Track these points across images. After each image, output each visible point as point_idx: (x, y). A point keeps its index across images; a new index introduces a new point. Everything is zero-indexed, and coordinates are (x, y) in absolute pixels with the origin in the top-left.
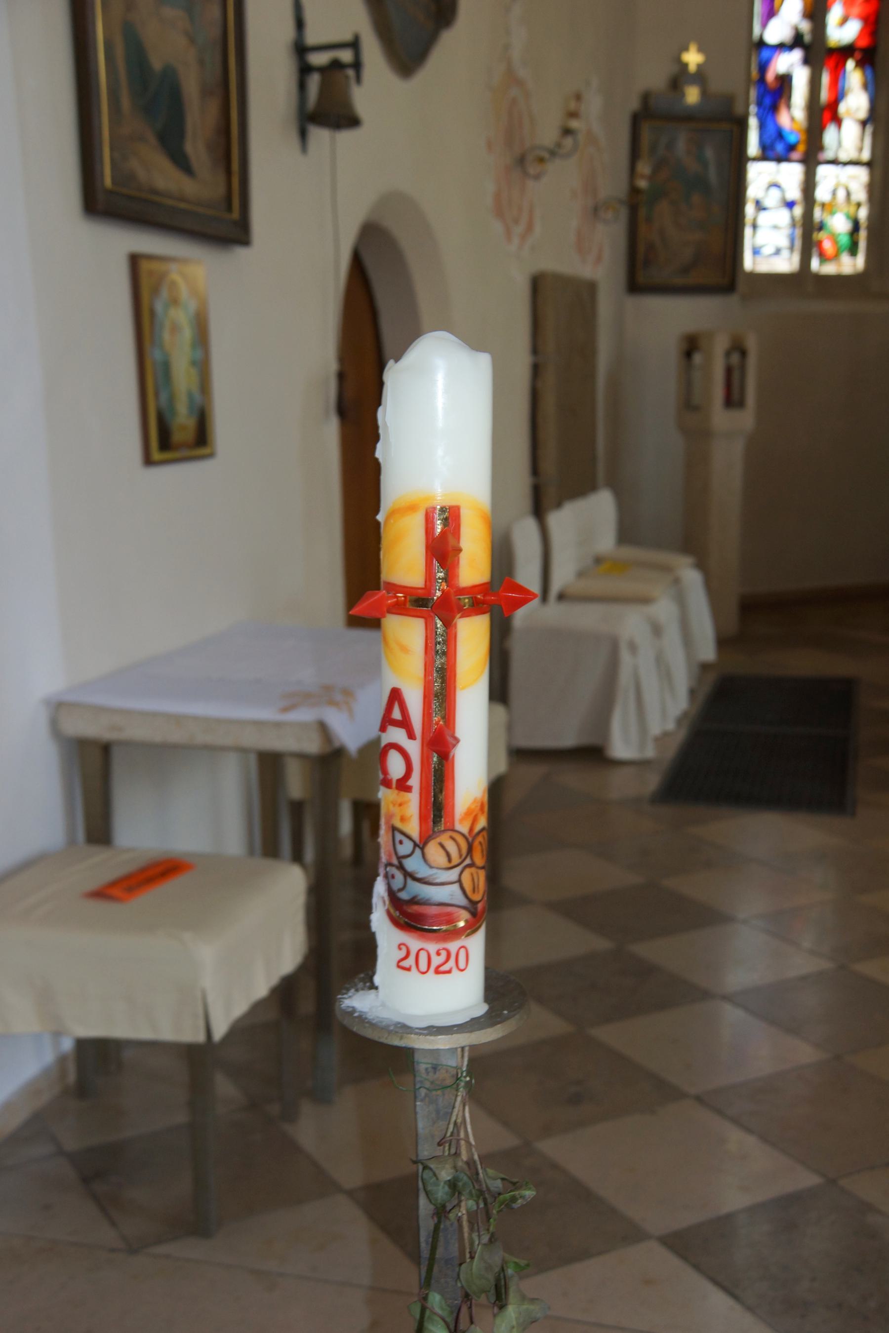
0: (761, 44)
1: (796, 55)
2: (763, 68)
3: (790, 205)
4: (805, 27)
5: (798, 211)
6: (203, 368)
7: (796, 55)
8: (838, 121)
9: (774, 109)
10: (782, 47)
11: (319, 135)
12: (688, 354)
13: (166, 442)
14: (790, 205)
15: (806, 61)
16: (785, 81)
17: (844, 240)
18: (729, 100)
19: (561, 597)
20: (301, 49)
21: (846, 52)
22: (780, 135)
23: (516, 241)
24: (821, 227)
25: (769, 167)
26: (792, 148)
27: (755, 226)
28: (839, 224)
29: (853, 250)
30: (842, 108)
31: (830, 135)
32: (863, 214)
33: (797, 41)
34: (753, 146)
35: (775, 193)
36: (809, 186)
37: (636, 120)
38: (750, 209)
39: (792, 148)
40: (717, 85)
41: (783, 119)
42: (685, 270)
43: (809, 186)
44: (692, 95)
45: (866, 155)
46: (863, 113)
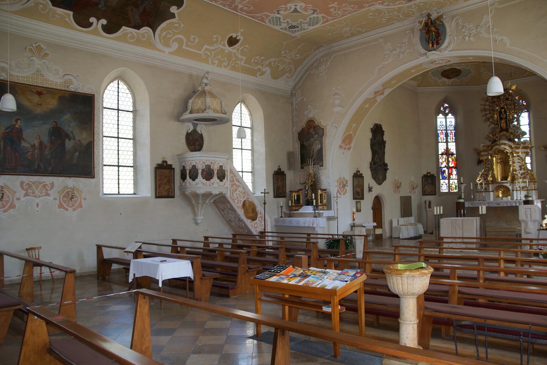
0: (441, 167)
1: (446, 168)
2: (441, 170)
3: (446, 184)
4: (447, 165)
5: (448, 185)
6: (361, 208)
7: (446, 168)
8: (452, 175)
9: (443, 174)
10: (444, 167)
11: (370, 192)
12: (425, 202)
13: (358, 211)
14: (446, 184)
15: (447, 169)
16: (444, 171)
17: (455, 188)
18: (433, 175)
19: (400, 225)
20: (369, 187)
21: (453, 167)
22: (444, 176)
23: (397, 194)
24: (451, 187)
25: (443, 181)
26: (446, 178)
27: (442, 187)
28: (454, 186)
29: (456, 189)
30: (453, 173)
31: (451, 176)
32: (457, 185)
33: (446, 167)
34: (441, 178)
35: (444, 183)
36: (449, 182)
37: (422, 177)
38: (441, 185)
39: (446, 178)
40: (432, 173)
41: (445, 175)
42: (430, 193)
43: (449, 182)
44: (429, 175)
45: (457, 178)
46: (456, 174)
